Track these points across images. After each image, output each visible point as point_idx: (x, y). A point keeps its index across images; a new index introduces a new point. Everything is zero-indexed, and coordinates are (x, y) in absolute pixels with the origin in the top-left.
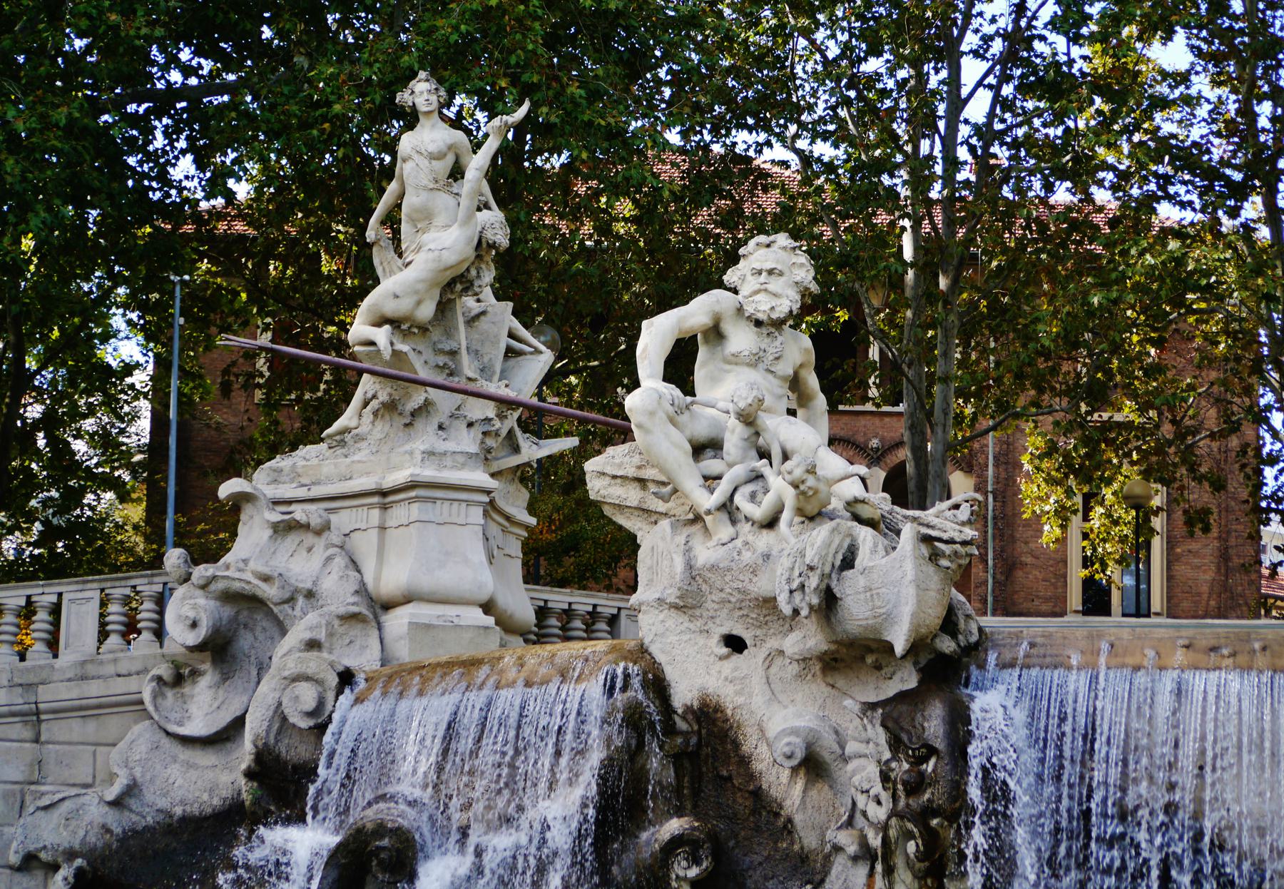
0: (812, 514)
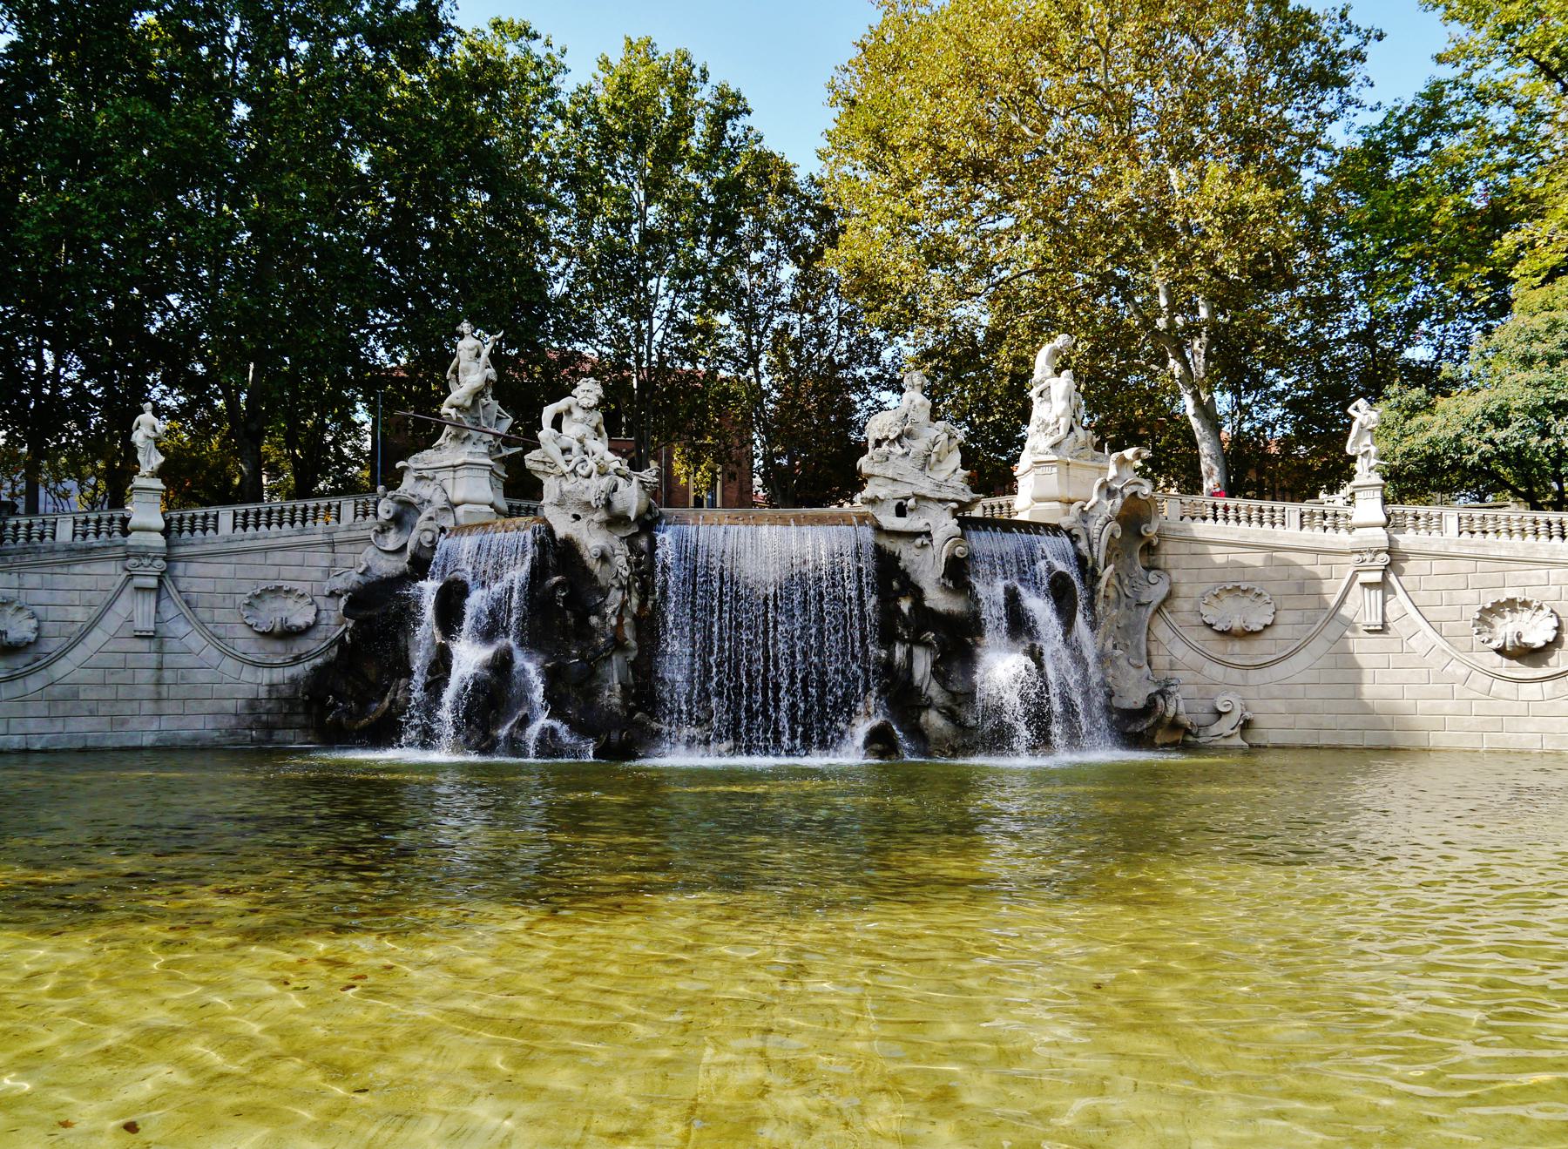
0: (603, 473)
